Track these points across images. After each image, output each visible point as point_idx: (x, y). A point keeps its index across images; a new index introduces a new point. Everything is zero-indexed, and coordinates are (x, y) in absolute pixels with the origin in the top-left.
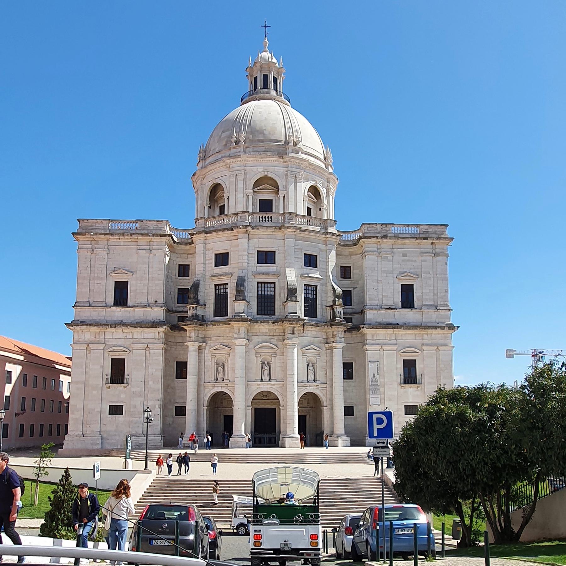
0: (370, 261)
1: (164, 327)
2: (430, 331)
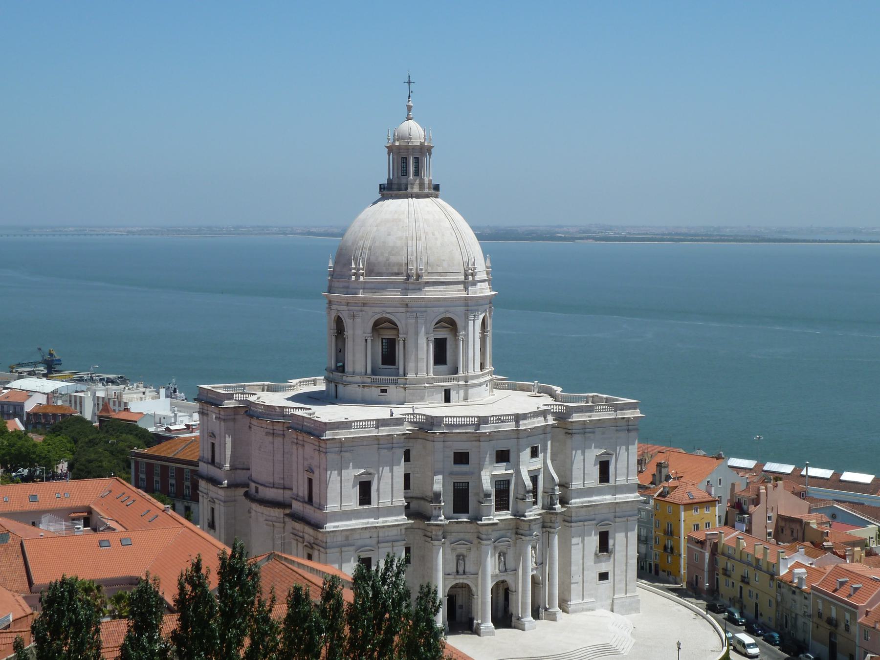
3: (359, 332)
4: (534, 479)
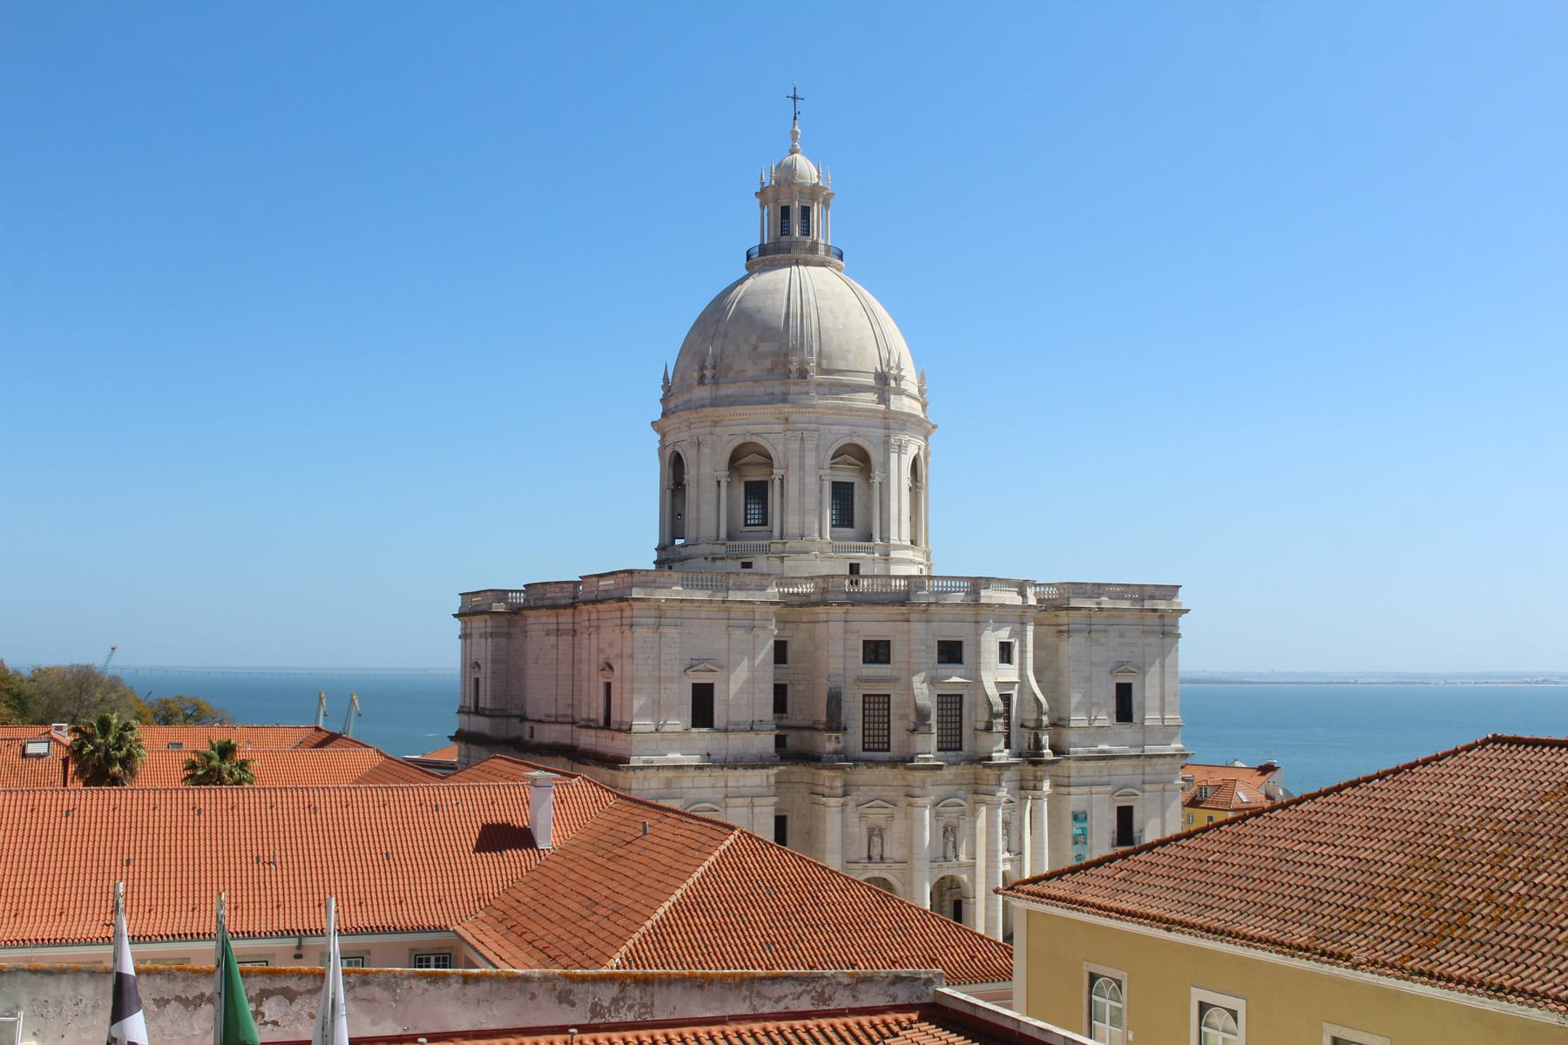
2: (1155, 761)
3: (707, 470)
4: (1007, 699)
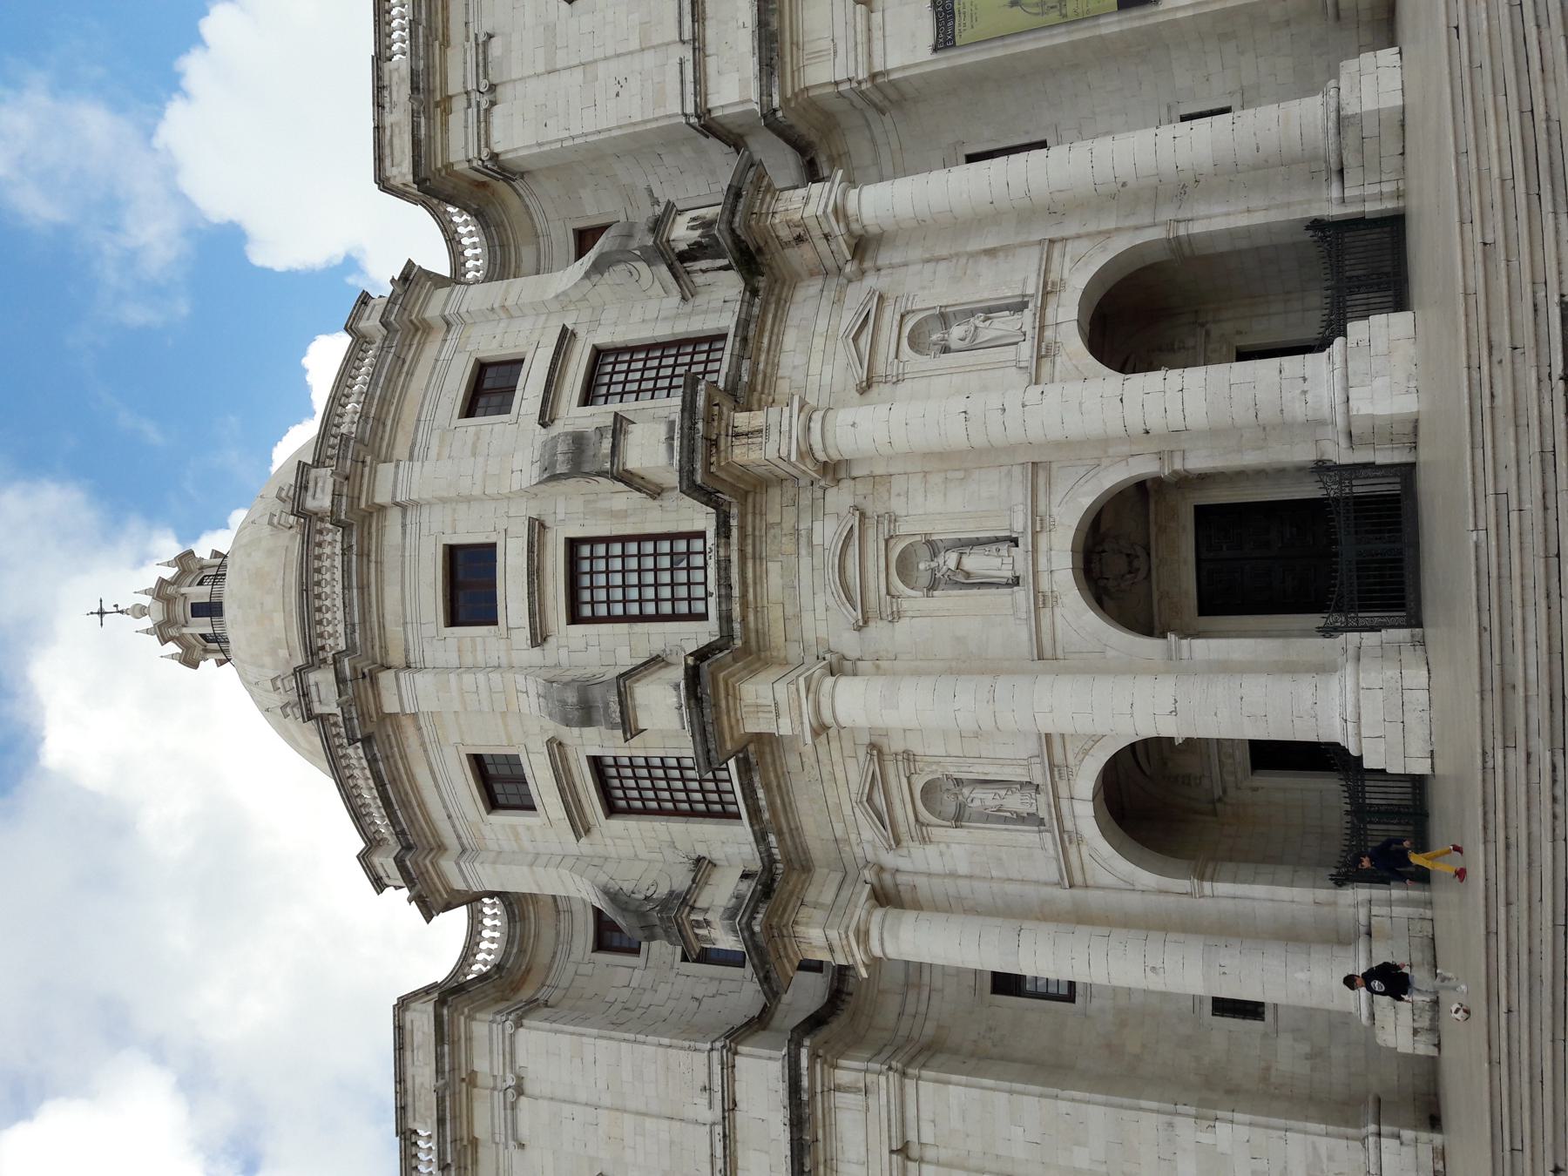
0: (515, 134)
1: (804, 1062)
